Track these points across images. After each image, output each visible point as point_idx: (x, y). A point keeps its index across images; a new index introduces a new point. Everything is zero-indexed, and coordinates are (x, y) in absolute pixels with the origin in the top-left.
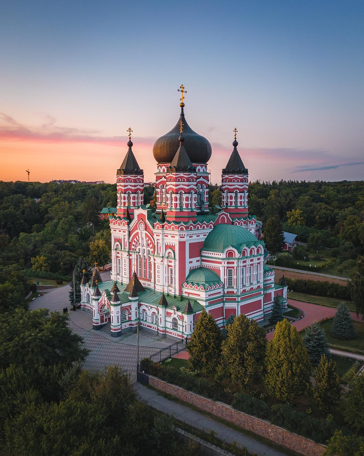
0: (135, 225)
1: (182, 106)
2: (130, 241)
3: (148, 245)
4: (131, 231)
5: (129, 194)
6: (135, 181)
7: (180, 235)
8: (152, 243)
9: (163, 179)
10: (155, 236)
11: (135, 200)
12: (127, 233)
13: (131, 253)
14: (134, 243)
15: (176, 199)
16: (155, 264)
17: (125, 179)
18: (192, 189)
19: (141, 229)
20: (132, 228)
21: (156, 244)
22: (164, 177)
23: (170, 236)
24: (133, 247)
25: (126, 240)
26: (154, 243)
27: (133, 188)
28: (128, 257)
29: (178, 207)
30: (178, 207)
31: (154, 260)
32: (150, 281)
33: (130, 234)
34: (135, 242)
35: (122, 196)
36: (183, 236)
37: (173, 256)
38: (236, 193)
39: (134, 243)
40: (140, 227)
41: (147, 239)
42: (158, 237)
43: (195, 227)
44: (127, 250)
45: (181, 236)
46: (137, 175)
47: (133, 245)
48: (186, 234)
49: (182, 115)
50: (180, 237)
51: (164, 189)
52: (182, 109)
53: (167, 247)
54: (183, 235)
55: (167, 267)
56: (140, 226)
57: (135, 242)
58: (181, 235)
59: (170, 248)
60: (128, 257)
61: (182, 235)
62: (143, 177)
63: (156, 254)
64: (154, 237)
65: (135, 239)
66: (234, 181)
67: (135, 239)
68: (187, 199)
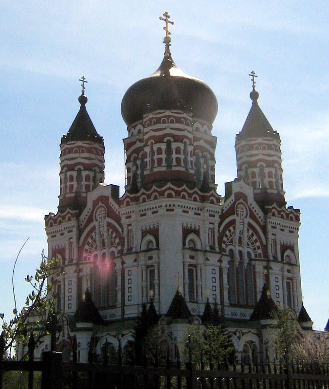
0: (89, 214)
3: (112, 244)
5: (79, 171)
6: (89, 150)
7: (166, 206)
8: (119, 235)
9: (138, 144)
10: (124, 221)
11: (89, 181)
12: (75, 230)
13: (81, 266)
14: (87, 247)
15: (160, 151)
19: (100, 220)
21: (125, 233)
22: (139, 140)
23: (149, 213)
25: (75, 245)
27: (87, 162)
28: (76, 274)
29: (164, 163)
30: (164, 163)
31: (123, 263)
32: (114, 307)
33: (80, 231)
34: (88, 244)
35: (68, 176)
36: (172, 207)
37: (155, 246)
44: (74, 262)
45: (168, 207)
50: (167, 210)
54: (172, 205)
55: (144, 268)
56: (98, 213)
57: (88, 244)
58: (168, 205)
60: (76, 274)
61: (170, 205)
64: (122, 222)
65: (90, 240)
66: (257, 149)
67: (90, 240)
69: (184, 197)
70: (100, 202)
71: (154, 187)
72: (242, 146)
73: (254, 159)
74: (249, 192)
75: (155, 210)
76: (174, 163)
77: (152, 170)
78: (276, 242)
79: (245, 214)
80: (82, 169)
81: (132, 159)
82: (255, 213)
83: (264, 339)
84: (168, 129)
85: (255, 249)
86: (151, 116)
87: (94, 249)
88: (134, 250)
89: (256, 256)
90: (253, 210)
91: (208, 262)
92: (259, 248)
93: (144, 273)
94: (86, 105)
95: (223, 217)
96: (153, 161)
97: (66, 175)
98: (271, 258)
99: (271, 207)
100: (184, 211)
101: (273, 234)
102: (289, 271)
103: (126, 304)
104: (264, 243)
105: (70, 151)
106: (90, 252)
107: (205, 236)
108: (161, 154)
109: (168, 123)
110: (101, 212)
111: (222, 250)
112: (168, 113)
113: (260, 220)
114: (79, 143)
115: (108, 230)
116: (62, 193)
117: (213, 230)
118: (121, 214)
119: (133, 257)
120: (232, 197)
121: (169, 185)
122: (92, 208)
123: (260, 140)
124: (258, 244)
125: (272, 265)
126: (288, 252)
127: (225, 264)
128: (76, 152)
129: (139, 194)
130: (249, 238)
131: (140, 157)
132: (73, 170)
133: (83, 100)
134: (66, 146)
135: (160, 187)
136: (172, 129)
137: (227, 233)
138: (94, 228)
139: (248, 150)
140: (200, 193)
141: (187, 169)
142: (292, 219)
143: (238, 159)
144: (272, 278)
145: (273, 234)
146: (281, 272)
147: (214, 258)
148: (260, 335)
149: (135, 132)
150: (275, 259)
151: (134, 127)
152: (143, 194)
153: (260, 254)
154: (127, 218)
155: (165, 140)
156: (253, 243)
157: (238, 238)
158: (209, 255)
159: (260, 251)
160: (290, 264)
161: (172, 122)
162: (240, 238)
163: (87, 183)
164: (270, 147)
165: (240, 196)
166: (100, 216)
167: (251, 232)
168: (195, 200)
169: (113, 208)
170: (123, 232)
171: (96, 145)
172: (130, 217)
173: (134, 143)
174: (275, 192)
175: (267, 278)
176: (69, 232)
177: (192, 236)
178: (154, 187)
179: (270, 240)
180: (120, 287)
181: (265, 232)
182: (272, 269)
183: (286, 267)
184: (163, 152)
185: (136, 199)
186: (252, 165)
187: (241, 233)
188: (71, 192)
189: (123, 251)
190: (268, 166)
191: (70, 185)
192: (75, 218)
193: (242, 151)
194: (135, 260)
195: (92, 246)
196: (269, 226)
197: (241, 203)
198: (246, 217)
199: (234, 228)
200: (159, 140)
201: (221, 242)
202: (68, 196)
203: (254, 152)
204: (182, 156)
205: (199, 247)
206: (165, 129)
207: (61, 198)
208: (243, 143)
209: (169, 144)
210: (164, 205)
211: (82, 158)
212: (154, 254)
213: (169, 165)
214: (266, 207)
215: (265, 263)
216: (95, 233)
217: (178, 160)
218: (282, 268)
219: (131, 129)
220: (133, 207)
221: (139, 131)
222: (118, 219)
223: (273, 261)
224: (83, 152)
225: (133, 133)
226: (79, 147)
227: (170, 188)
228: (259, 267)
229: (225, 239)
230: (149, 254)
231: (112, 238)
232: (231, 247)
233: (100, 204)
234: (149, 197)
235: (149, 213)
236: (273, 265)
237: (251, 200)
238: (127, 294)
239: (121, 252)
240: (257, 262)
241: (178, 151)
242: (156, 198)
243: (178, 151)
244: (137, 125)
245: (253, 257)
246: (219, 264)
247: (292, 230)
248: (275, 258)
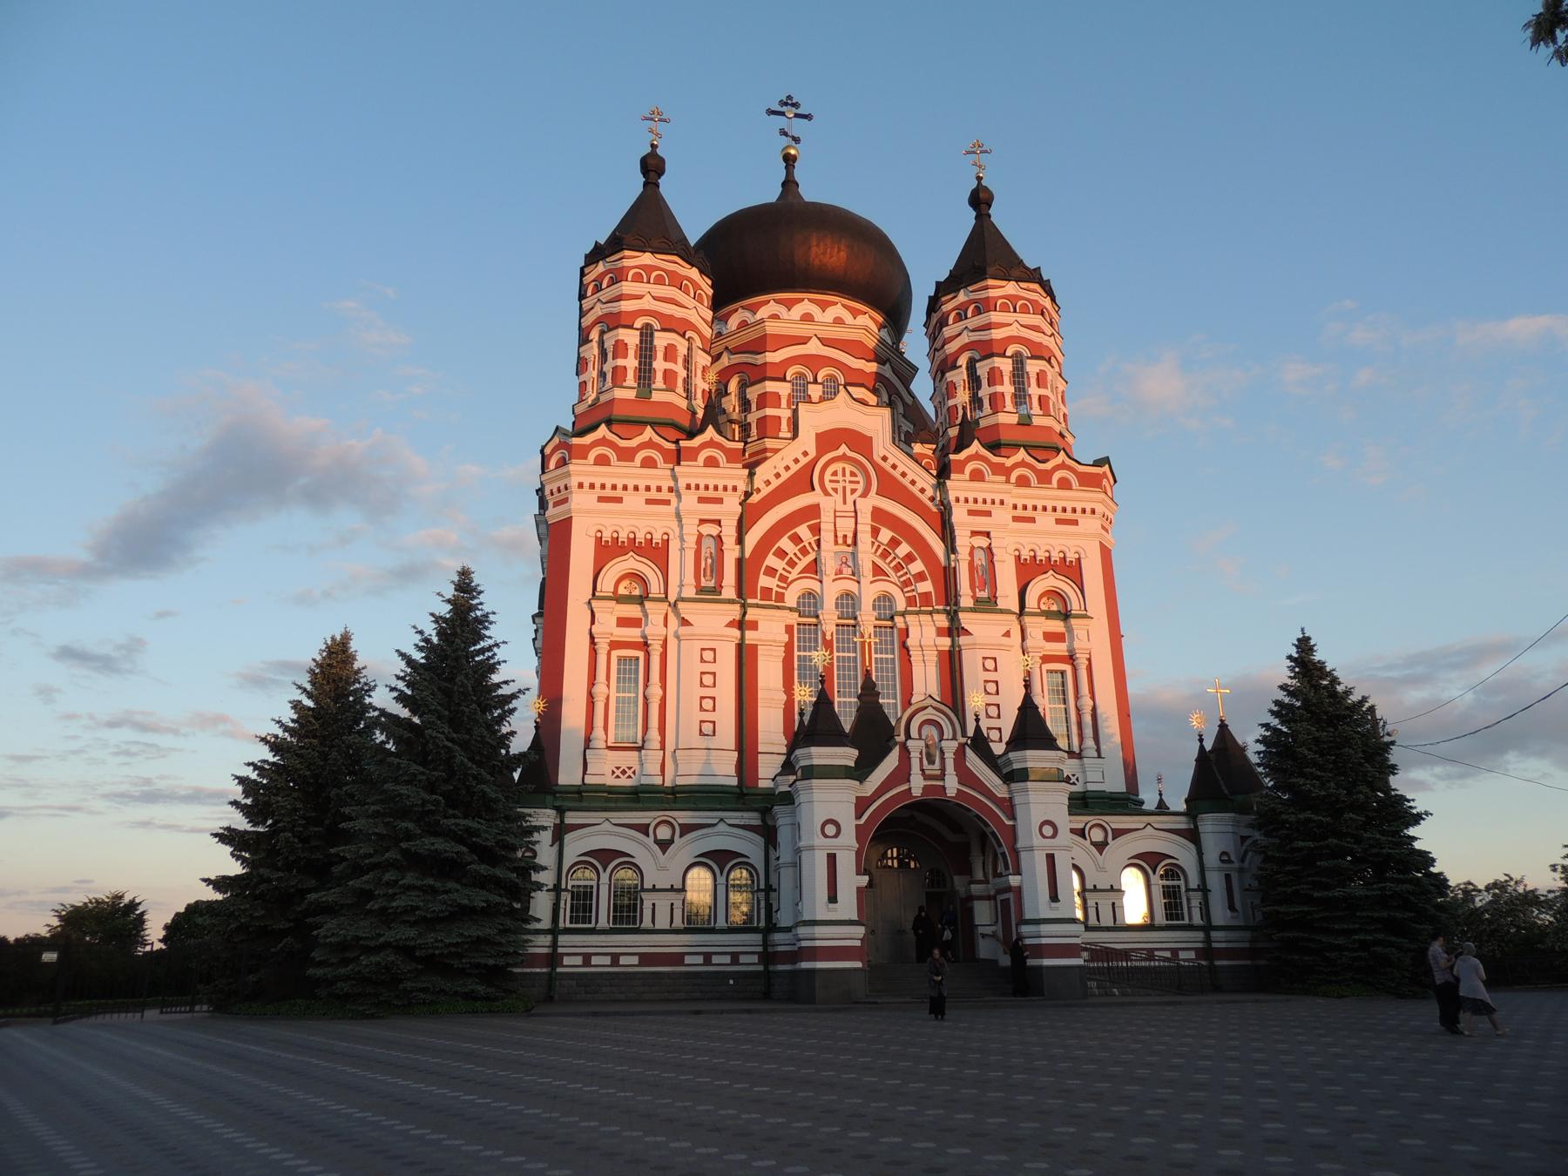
38: (1018, 361)
68: (670, 353)
89: (911, 601)
102: (1050, 637)
109: (649, 282)
136: (655, 298)
150: (987, 605)
153: (926, 597)
175: (951, 664)
181: (946, 531)
182: (970, 634)
183: (1037, 627)
209: (647, 334)
215: (942, 621)
217: (669, 376)
228: (926, 634)
236: (966, 619)
240: (908, 618)
245: (901, 605)
248: (987, 605)
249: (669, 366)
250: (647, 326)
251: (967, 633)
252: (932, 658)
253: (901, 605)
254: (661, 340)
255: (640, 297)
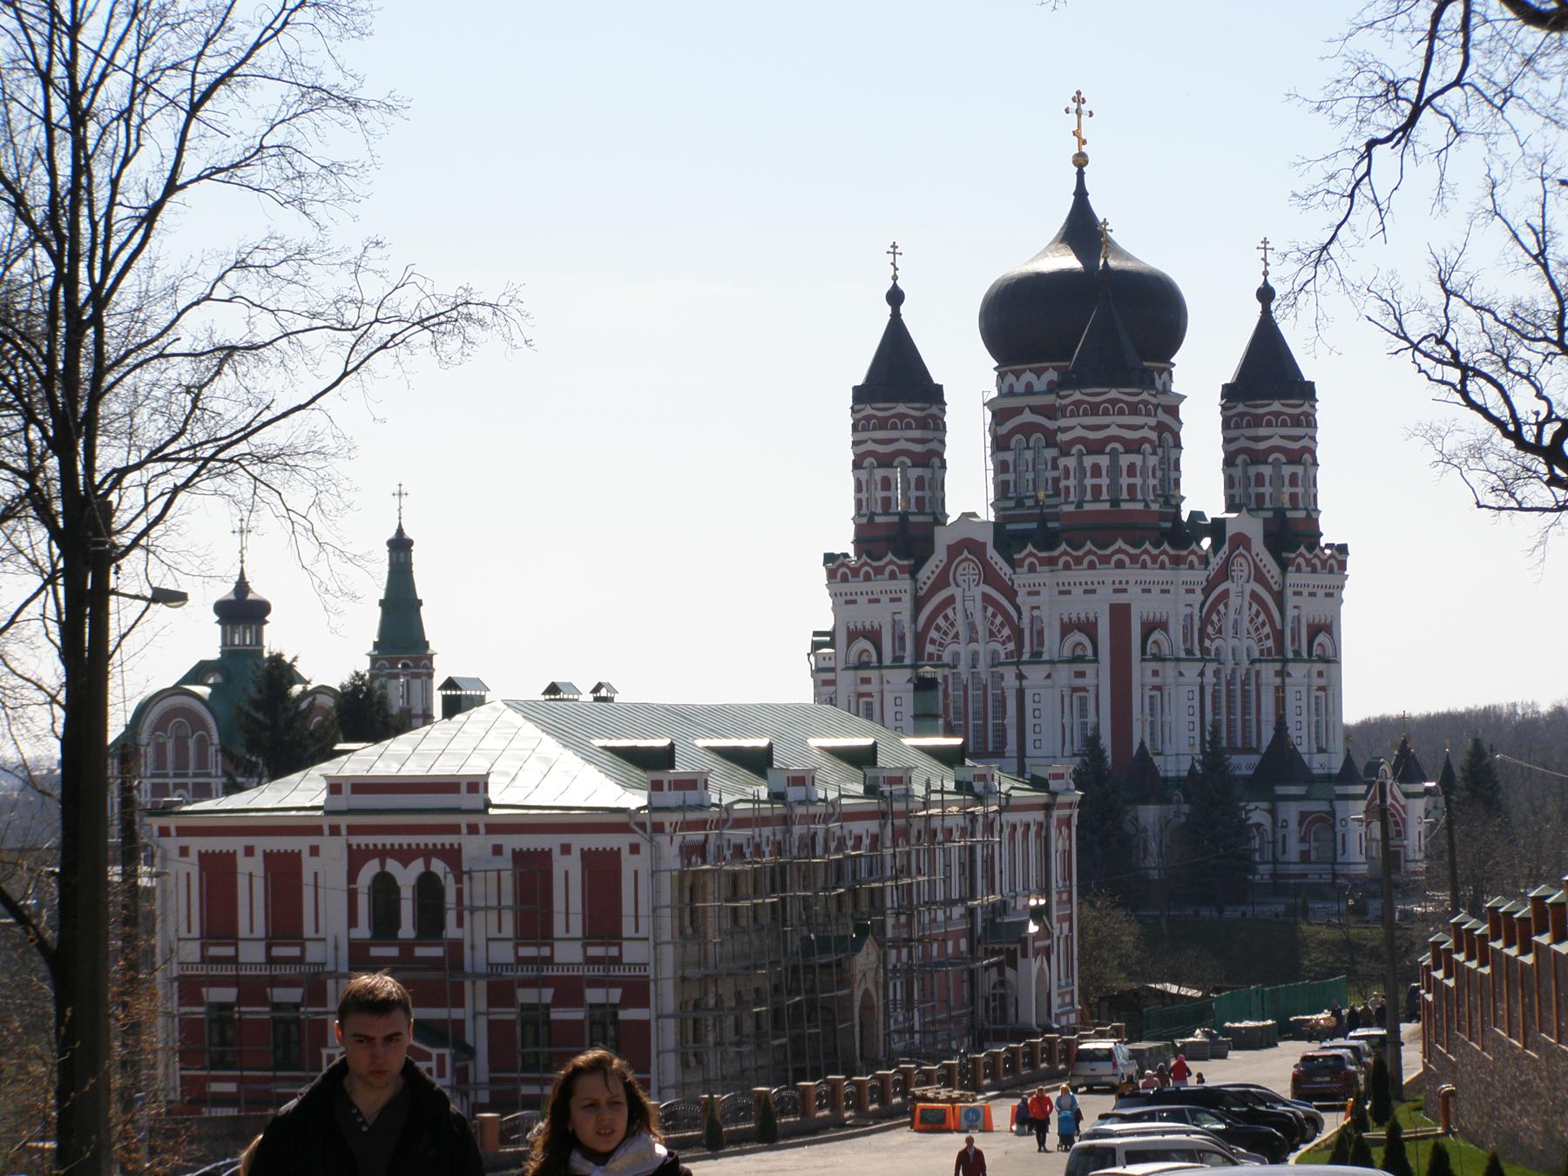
0: (937, 571)
1: (1081, 161)
2: (920, 627)
3: (992, 634)
4: (922, 593)
6: (923, 424)
9: (1028, 417)
15: (1096, 470)
16: (1021, 694)
17: (887, 419)
18: (1144, 440)
20: (929, 583)
23: (1077, 591)
24: (930, 648)
26: (1016, 618)
27: (917, 448)
29: (1105, 496)
31: (1021, 677)
33: (918, 603)
34: (938, 628)
36: (1123, 586)
39: (933, 634)
40: (960, 579)
41: (990, 610)
42: (1034, 600)
43: (1154, 559)
44: (908, 661)
45: (1117, 586)
46: (925, 402)
47: (933, 641)
48: (1132, 581)
49: (1081, 194)
50: (1116, 591)
51: (1031, 452)
52: (1080, 175)
53: (1067, 628)
55: (1067, 693)
56: (960, 571)
57: (938, 628)
59: (1080, 631)
61: (1120, 582)
62: (944, 411)
63: (1026, 657)
64: (1019, 600)
66: (1269, 424)
69: (1144, 566)
70: (966, 552)
71: (1089, 545)
72: (1238, 415)
73: (1262, 446)
74: (1253, 528)
75: (1090, 587)
76: (1125, 496)
77: (1080, 504)
78: (1299, 621)
79: (1245, 575)
80: (909, 463)
81: (1012, 445)
82: (1265, 571)
83: (1281, 817)
84: (1113, 427)
85: (1260, 640)
86: (1077, 396)
87: (949, 639)
88: (1045, 657)
89: (1262, 652)
90: (1261, 565)
91: (1181, 679)
92: (1267, 637)
93: (1067, 700)
94: (903, 309)
95: (1207, 592)
96: (1083, 488)
97: (871, 474)
98: (1290, 655)
99: (1293, 555)
100: (1144, 591)
101: (1295, 607)
102: (1320, 674)
103: (1028, 754)
104: (1279, 626)
105: (882, 424)
106: (941, 645)
107: (1176, 629)
108: (1100, 476)
110: (967, 571)
111: (1204, 651)
112: (1113, 393)
113: (1272, 582)
114: (901, 408)
115: (985, 609)
116: (864, 511)
117: (1191, 616)
118: (1016, 586)
119: (1046, 669)
120: (1226, 548)
121: (1120, 544)
122: (945, 560)
123: (1276, 406)
124: (1267, 629)
125: (1291, 667)
126: (1322, 638)
127: (1209, 678)
128: (894, 427)
129: (1056, 553)
130: (1252, 620)
131: (1031, 445)
132: (890, 465)
133: (895, 297)
134: (869, 411)
135: (1106, 547)
137: (1215, 617)
138: (950, 600)
139: (1249, 426)
140: (1172, 552)
141: (1147, 505)
142: (1331, 571)
143: (1227, 441)
144: (1290, 694)
145: (1295, 607)
146: (1306, 680)
147: (1191, 670)
148: (1272, 812)
149: (1020, 387)
151: (1018, 375)
152: (1065, 553)
154: (1030, 594)
155: (1107, 450)
156: (1257, 629)
157: (1231, 624)
158: (1184, 666)
159: (1270, 643)
160: (1324, 659)
161: (1121, 412)
162: (1236, 620)
163: (920, 493)
164: (1296, 421)
165: (1242, 540)
166: (966, 578)
167: (1255, 607)
168: (1162, 567)
169: (997, 568)
170: (1020, 618)
171: (934, 410)
172: (1037, 593)
173: (1018, 411)
174: (1301, 514)
176: (892, 600)
177: (1157, 635)
178: (1089, 545)
179: (1289, 619)
180: (1014, 720)
184: (1104, 472)
185: (1052, 562)
186: (1258, 458)
187: (1239, 612)
188: (886, 513)
189: (1020, 654)
190: (1290, 462)
191: (883, 499)
192: (907, 576)
193: (1237, 426)
194: (1049, 676)
195: (946, 633)
196: (1289, 592)
197: (1241, 555)
198: (1248, 582)
199: (1226, 606)
200: (1095, 448)
201: (1203, 634)
202: (879, 520)
203: (1262, 431)
204: (1138, 481)
205: (1166, 651)
206: (1108, 426)
207: (864, 520)
208: (1241, 408)
209: (1114, 454)
210: (1109, 581)
211: (905, 439)
212: (1089, 669)
213: (1115, 502)
214: (1284, 555)
215: (1278, 666)
216: (954, 609)
218: (1309, 672)
219: (1006, 373)
220: (1043, 576)
221: (1029, 386)
222: (1011, 594)
223: (1294, 661)
224: (909, 427)
225: (1011, 386)
226: (902, 416)
227: (1120, 551)
229: (1210, 629)
230: (1079, 667)
231: (992, 623)
232: (1218, 642)
233: (966, 553)
234: (1078, 561)
235: (1077, 591)
236: (1291, 667)
237: (1258, 545)
238: (1030, 736)
239: (1015, 658)
240: (1264, 665)
241: (1132, 470)
242: (1092, 566)
243: (1132, 470)
244: (1024, 371)
246: (1199, 679)
247: (1331, 591)
248: (1297, 653)
249: (1132, 480)
250: (1113, 449)
251: (1289, 675)
252: (1272, 690)
253: (1256, 655)
254: (1125, 460)
255: (1108, 426)
